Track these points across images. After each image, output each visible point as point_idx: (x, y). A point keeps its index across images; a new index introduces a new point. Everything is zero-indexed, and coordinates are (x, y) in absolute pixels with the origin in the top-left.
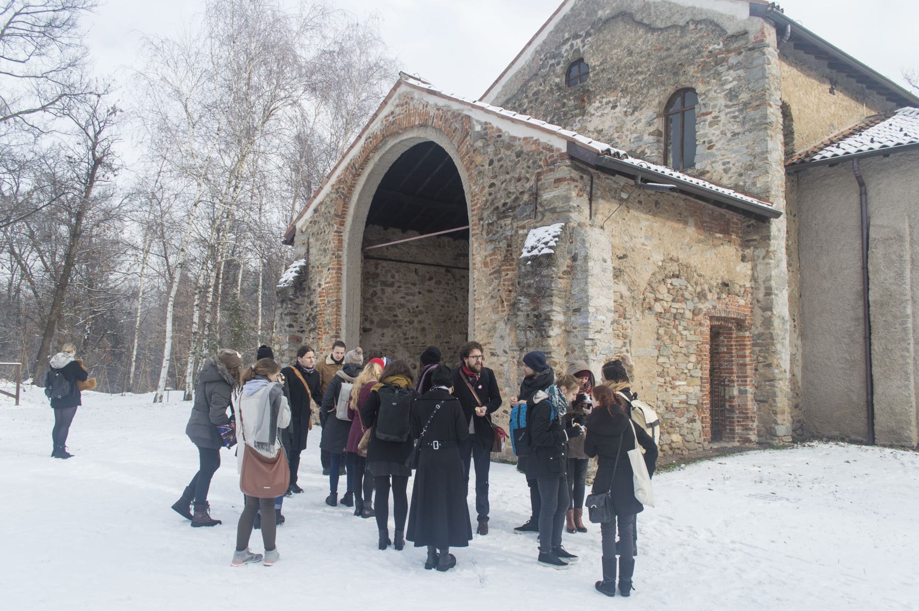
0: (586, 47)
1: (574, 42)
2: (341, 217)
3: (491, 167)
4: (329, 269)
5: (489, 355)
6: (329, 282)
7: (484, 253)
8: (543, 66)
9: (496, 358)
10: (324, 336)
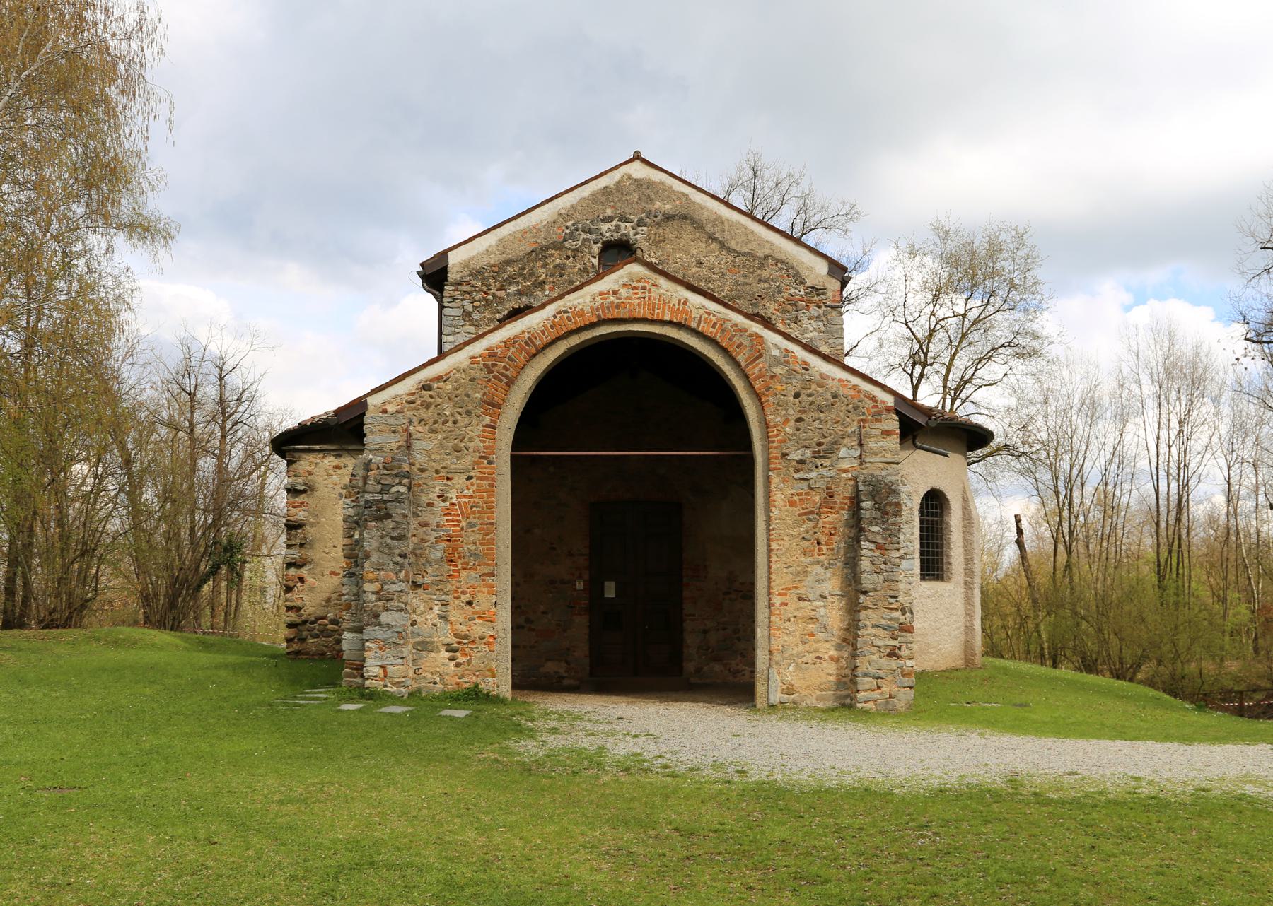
3: (797, 400)
4: (470, 478)
6: (471, 496)
7: (788, 491)
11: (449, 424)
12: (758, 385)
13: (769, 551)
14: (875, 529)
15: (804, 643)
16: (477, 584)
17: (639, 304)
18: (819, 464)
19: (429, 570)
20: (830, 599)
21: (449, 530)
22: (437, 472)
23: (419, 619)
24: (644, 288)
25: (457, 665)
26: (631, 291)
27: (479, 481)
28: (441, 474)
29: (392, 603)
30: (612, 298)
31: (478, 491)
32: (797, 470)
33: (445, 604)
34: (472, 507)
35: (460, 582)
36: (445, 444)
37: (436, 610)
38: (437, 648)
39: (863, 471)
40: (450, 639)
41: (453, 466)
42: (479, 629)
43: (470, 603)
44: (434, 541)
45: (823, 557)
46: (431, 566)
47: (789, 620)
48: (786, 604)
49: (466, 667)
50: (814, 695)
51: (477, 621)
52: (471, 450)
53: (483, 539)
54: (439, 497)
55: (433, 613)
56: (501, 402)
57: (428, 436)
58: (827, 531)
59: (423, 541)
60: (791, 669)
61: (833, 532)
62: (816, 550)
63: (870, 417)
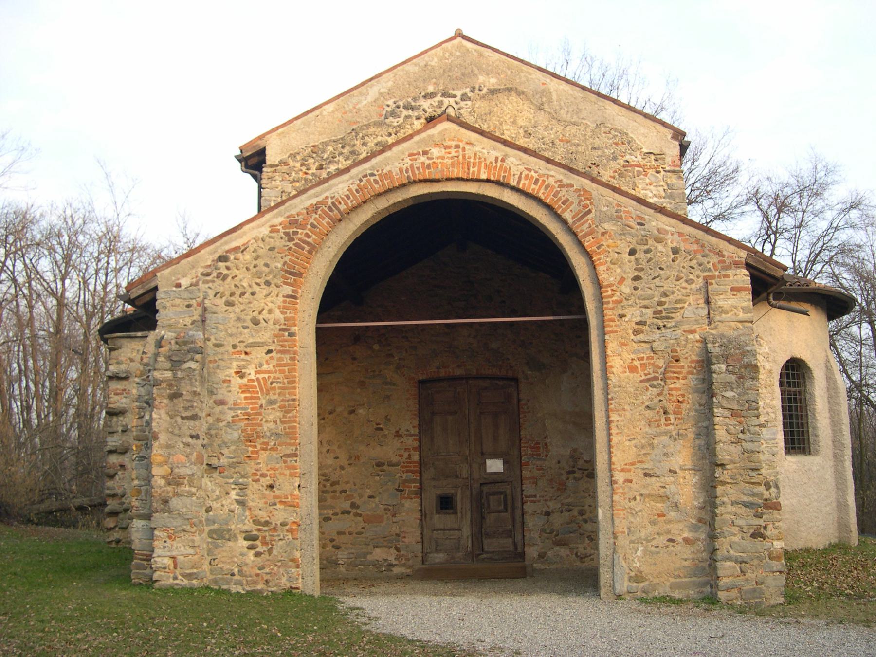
0: (462, 111)
1: (446, 101)
2: (293, 274)
3: (632, 257)
5: (643, 476)
6: (269, 372)
7: (628, 357)
8: (393, 114)
9: (654, 479)
10: (263, 455)
11: (247, 295)
12: (588, 242)
13: (609, 422)
14: (729, 394)
15: (653, 523)
16: (278, 466)
17: (453, 165)
18: (661, 324)
19: (225, 451)
20: (681, 473)
21: (247, 409)
22: (234, 346)
23: (215, 505)
24: (457, 147)
25: (257, 555)
26: (443, 150)
27: (279, 355)
28: (239, 349)
29: (182, 488)
30: (423, 159)
31: (279, 365)
32: (636, 332)
33: (243, 487)
34: (271, 383)
35: (259, 463)
36: (243, 317)
37: (233, 494)
38: (235, 536)
39: (713, 332)
40: (249, 526)
41: (251, 340)
42: (280, 515)
43: (271, 487)
44: (230, 419)
45: (671, 427)
46: (228, 447)
47: (635, 499)
48: (631, 481)
49: (266, 556)
50: (668, 584)
51: (278, 506)
52: (271, 322)
53: (284, 417)
54: (237, 373)
55: (230, 498)
56: (302, 270)
57: (225, 309)
58: (674, 398)
59: (218, 420)
60: (639, 553)
61: (681, 399)
62: (663, 420)
63: (717, 273)
